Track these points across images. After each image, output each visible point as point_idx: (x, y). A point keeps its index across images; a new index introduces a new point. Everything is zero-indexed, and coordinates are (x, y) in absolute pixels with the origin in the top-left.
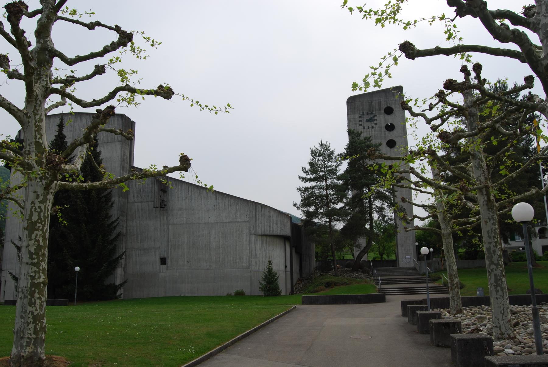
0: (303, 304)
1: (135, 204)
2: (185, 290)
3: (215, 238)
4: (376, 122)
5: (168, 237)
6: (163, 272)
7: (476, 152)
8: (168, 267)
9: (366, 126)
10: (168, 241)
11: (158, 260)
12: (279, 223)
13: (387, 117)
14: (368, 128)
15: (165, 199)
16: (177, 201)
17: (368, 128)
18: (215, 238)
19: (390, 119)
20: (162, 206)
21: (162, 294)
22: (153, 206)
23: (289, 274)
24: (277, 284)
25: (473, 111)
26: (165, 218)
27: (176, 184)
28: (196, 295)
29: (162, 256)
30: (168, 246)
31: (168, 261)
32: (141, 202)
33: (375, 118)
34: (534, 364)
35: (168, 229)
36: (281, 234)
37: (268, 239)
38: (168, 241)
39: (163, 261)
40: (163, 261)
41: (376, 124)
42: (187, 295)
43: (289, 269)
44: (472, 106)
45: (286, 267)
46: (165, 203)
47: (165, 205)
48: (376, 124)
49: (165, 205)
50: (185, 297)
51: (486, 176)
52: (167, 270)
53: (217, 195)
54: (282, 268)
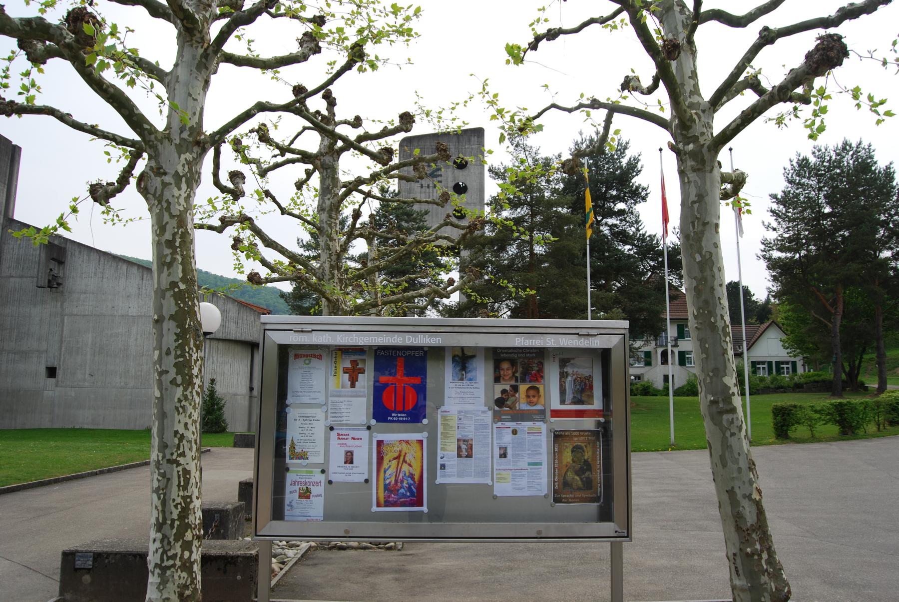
0: (235, 446)
1: (12, 280)
2: (84, 418)
3: (136, 339)
4: (440, 179)
5: (62, 336)
6: (51, 389)
7: (325, 225)
8: (58, 381)
9: (425, 185)
10: (61, 342)
11: (43, 370)
12: (240, 321)
13: (458, 172)
14: (428, 187)
15: (61, 274)
16: (80, 277)
17: (428, 187)
18: (136, 339)
19: (462, 177)
20: (54, 284)
21: (46, 424)
22: (35, 284)
23: (256, 402)
24: (221, 415)
25: (327, 161)
26: (59, 304)
27: (80, 252)
28: (101, 427)
29: (50, 365)
30: (61, 349)
31: (59, 373)
32: (21, 277)
33: (439, 173)
34: (116, 554)
35: (63, 321)
36: (243, 338)
37: (221, 345)
38: (61, 342)
39: (52, 372)
40: (52, 372)
41: (440, 182)
42: (86, 427)
43: (256, 392)
44: (326, 153)
45: (251, 389)
46: (60, 281)
47: (59, 284)
48: (440, 182)
49: (59, 284)
50: (81, 430)
51: (332, 263)
52: (57, 386)
53: (145, 273)
54: (243, 389)
